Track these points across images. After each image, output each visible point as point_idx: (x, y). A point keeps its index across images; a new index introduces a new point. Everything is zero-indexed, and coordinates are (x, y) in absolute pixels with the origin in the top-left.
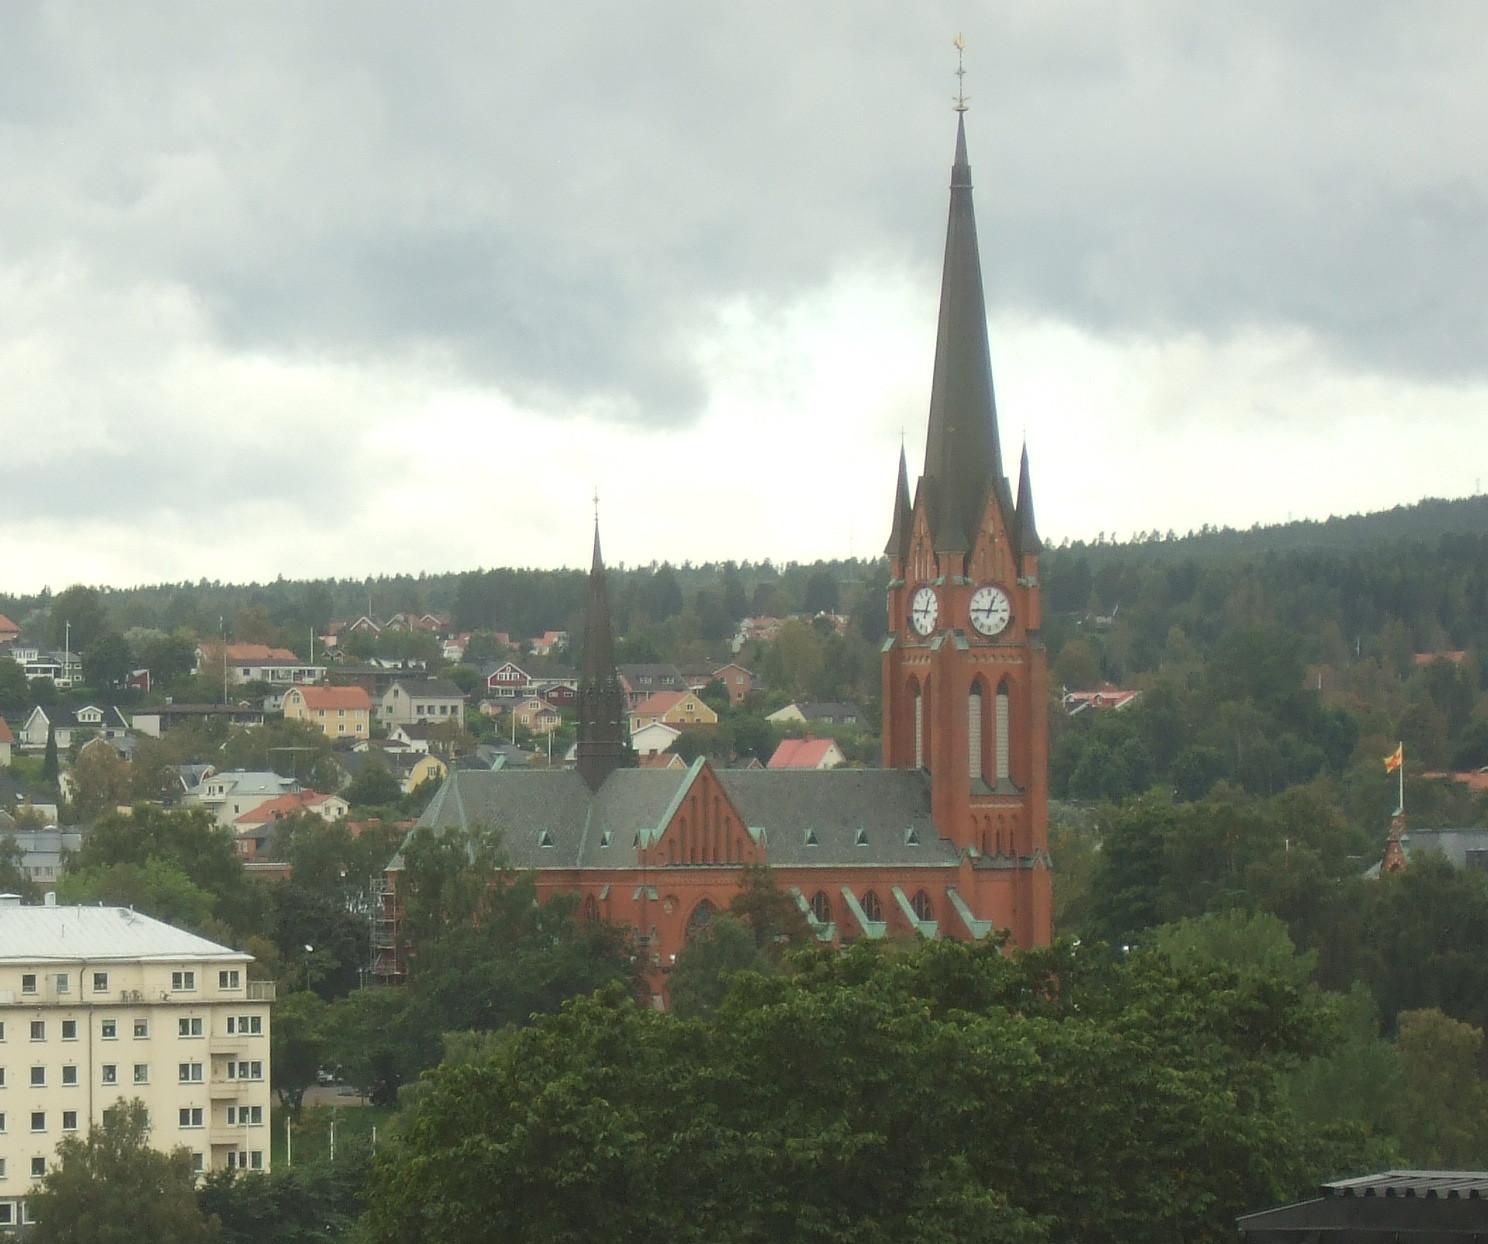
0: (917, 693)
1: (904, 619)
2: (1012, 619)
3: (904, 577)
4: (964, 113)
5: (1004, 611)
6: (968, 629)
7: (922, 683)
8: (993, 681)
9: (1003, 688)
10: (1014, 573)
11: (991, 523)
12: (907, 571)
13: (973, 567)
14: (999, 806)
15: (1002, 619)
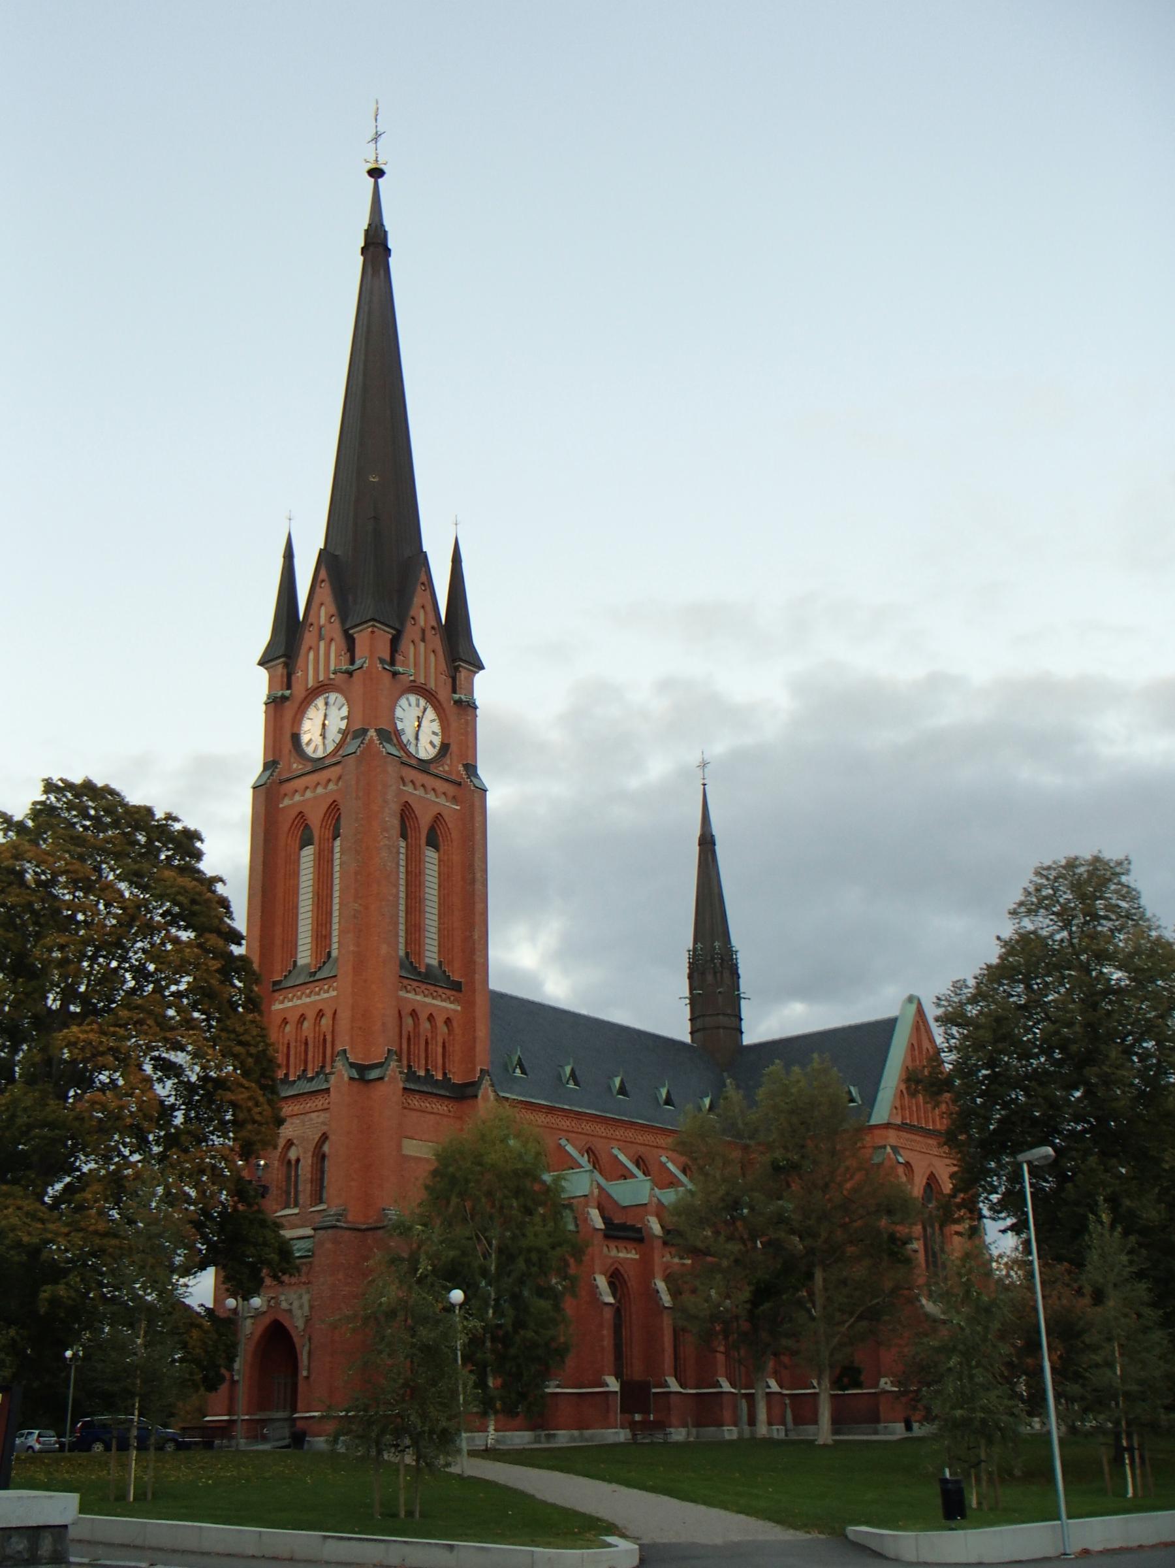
0: (306, 841)
1: (288, 745)
2: (444, 748)
3: (289, 687)
4: (380, 181)
5: (434, 733)
6: (390, 735)
7: (315, 819)
8: (425, 821)
9: (433, 842)
10: (449, 687)
11: (422, 612)
12: (293, 678)
13: (399, 658)
14: (429, 1000)
15: (431, 743)
